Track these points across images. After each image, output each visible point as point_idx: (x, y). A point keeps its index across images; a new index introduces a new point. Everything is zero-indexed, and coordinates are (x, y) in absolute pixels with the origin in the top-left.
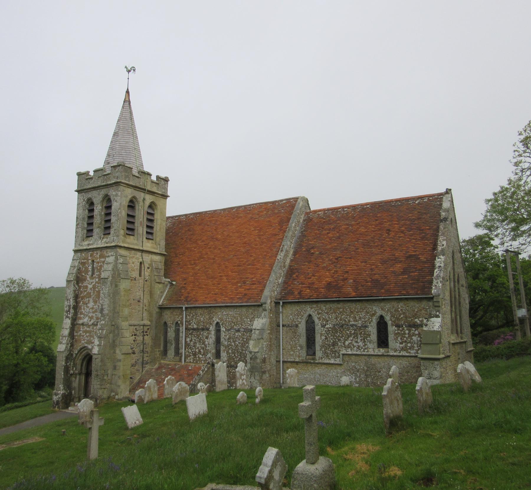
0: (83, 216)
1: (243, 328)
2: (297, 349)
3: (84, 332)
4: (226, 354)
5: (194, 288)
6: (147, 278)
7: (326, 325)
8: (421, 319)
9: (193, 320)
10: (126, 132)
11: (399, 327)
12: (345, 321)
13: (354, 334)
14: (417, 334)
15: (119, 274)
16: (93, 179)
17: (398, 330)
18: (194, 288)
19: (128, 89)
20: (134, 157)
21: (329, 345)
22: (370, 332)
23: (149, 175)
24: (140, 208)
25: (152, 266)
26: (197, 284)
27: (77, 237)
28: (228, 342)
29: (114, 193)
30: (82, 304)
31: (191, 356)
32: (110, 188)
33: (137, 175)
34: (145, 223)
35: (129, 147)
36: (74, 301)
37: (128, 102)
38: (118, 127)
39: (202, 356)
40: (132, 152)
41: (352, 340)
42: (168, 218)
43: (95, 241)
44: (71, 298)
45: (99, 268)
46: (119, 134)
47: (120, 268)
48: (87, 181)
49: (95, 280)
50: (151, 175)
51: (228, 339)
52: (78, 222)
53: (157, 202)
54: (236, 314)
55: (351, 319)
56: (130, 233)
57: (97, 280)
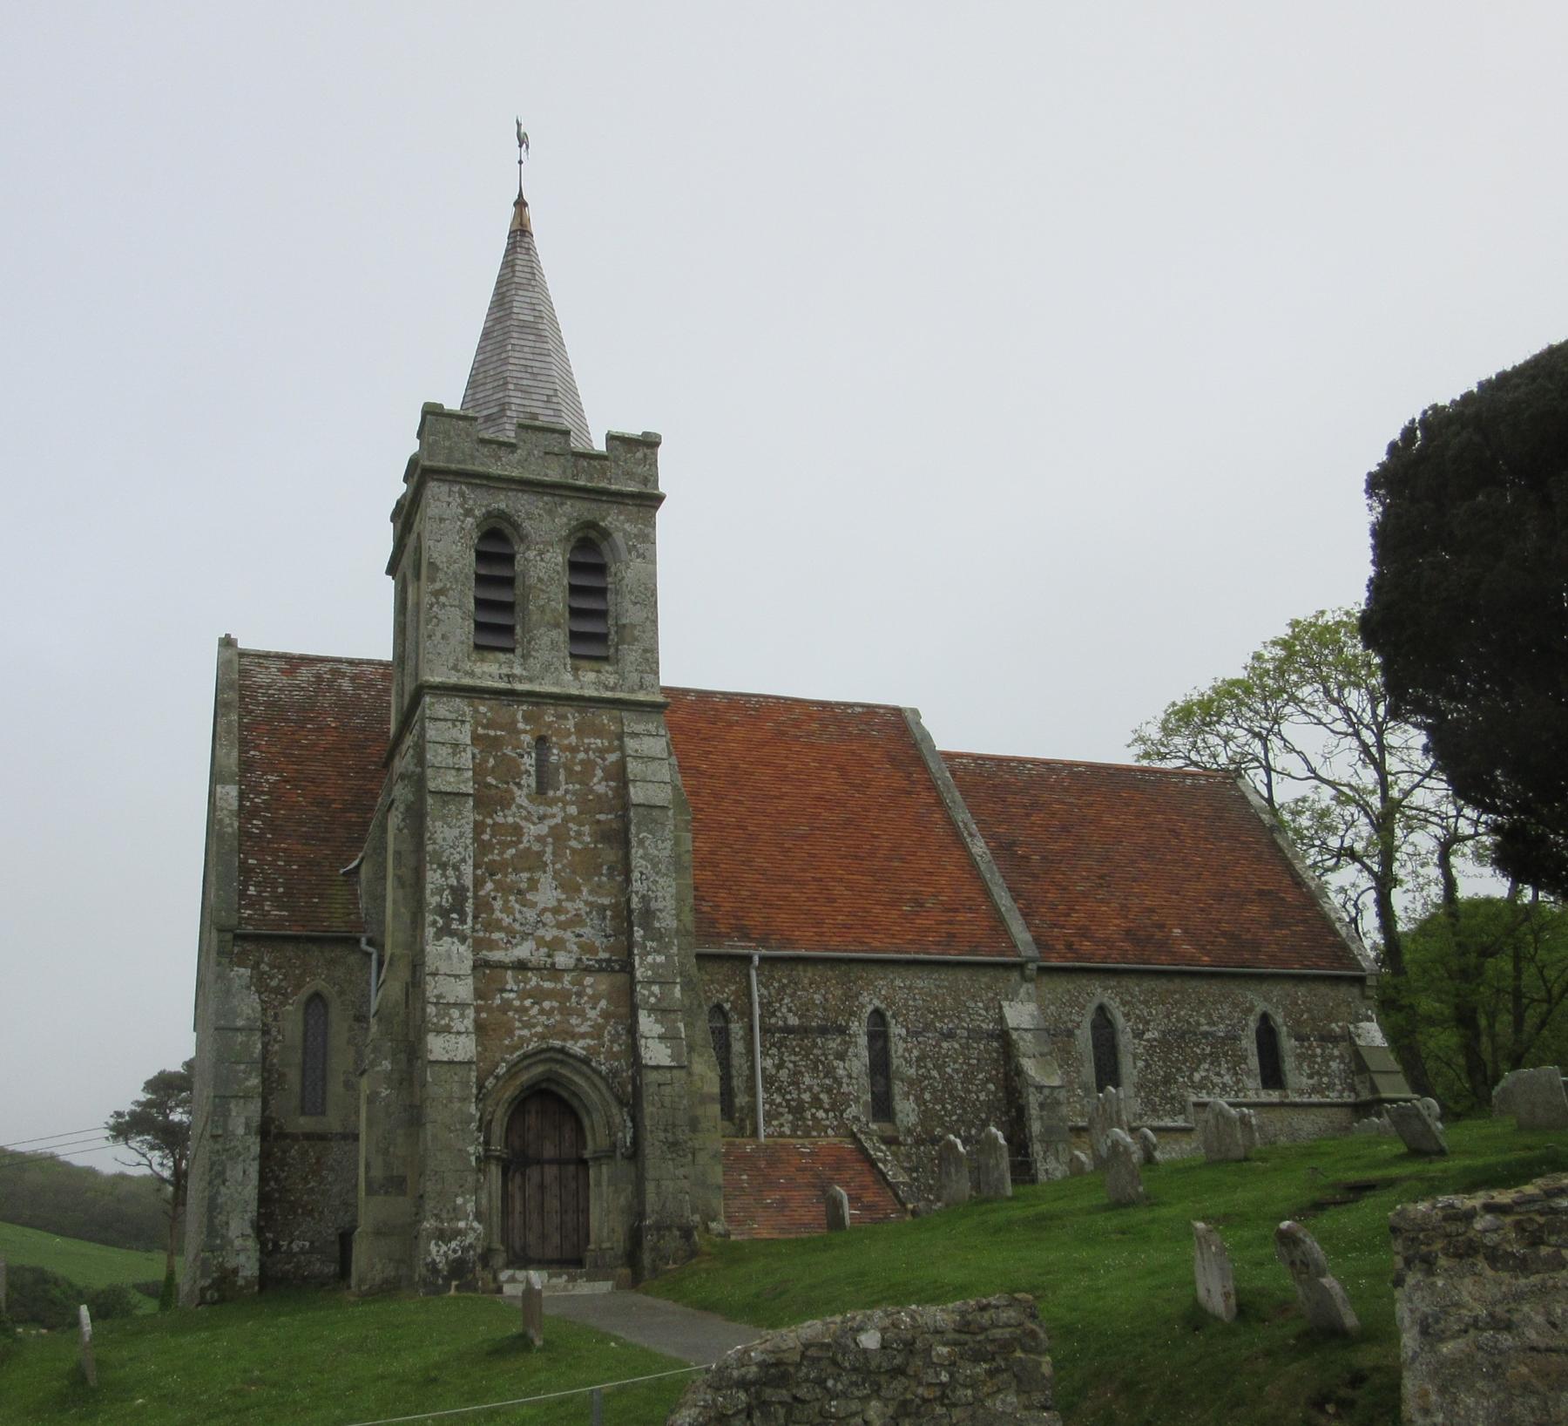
1: (963, 1028)
2: (1075, 1095)
3: (523, 995)
4: (913, 1105)
7: (1143, 1033)
8: (1340, 1024)
9: (783, 999)
11: (1303, 1041)
12: (1189, 1023)
13: (1211, 1054)
14: (1337, 1057)
17: (1302, 1046)
21: (1155, 1083)
22: (1246, 1050)
28: (919, 1067)
30: (496, 890)
31: (782, 1114)
39: (824, 1115)
41: (1207, 1070)
51: (919, 1059)
54: (938, 987)
55: (1203, 1020)
57: (573, 810)
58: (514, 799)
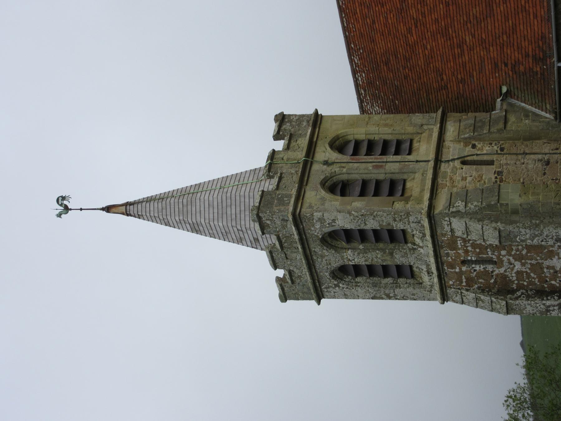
0: (371, 285)
5: (515, 44)
6: (495, 147)
10: (189, 207)
15: (489, 207)
16: (291, 269)
18: (515, 44)
19: (103, 209)
20: (239, 189)
23: (273, 154)
24: (345, 170)
25: (470, 138)
26: (505, 38)
27: (415, 297)
29: (318, 226)
30: (556, 281)
32: (308, 235)
33: (275, 181)
34: (376, 158)
35: (220, 201)
36: (549, 298)
37: (128, 207)
38: (180, 225)
40: (229, 194)
42: (363, 110)
43: (420, 260)
44: (544, 304)
45: (478, 250)
46: (194, 221)
47: (476, 206)
48: (298, 281)
49: (504, 256)
50: (274, 150)
52: (383, 296)
53: (331, 135)
56: (400, 188)
57: (503, 252)
58: (502, 274)
